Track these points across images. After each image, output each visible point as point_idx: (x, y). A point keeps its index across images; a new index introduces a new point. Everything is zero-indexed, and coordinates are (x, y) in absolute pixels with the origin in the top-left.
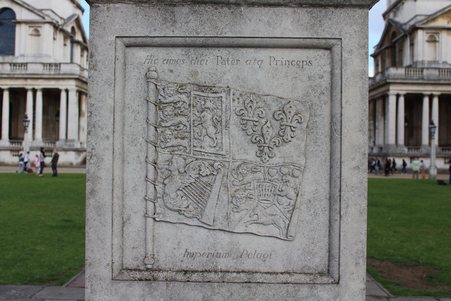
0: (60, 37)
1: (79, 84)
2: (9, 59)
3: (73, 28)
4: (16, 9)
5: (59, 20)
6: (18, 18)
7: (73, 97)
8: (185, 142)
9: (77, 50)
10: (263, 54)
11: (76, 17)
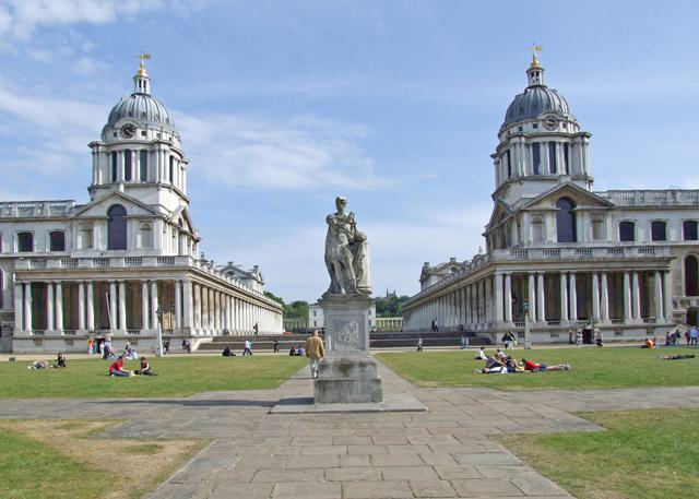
0: (169, 230)
2: (120, 253)
3: (180, 220)
4: (127, 206)
5: (167, 213)
6: (129, 214)
7: (188, 288)
9: (185, 239)
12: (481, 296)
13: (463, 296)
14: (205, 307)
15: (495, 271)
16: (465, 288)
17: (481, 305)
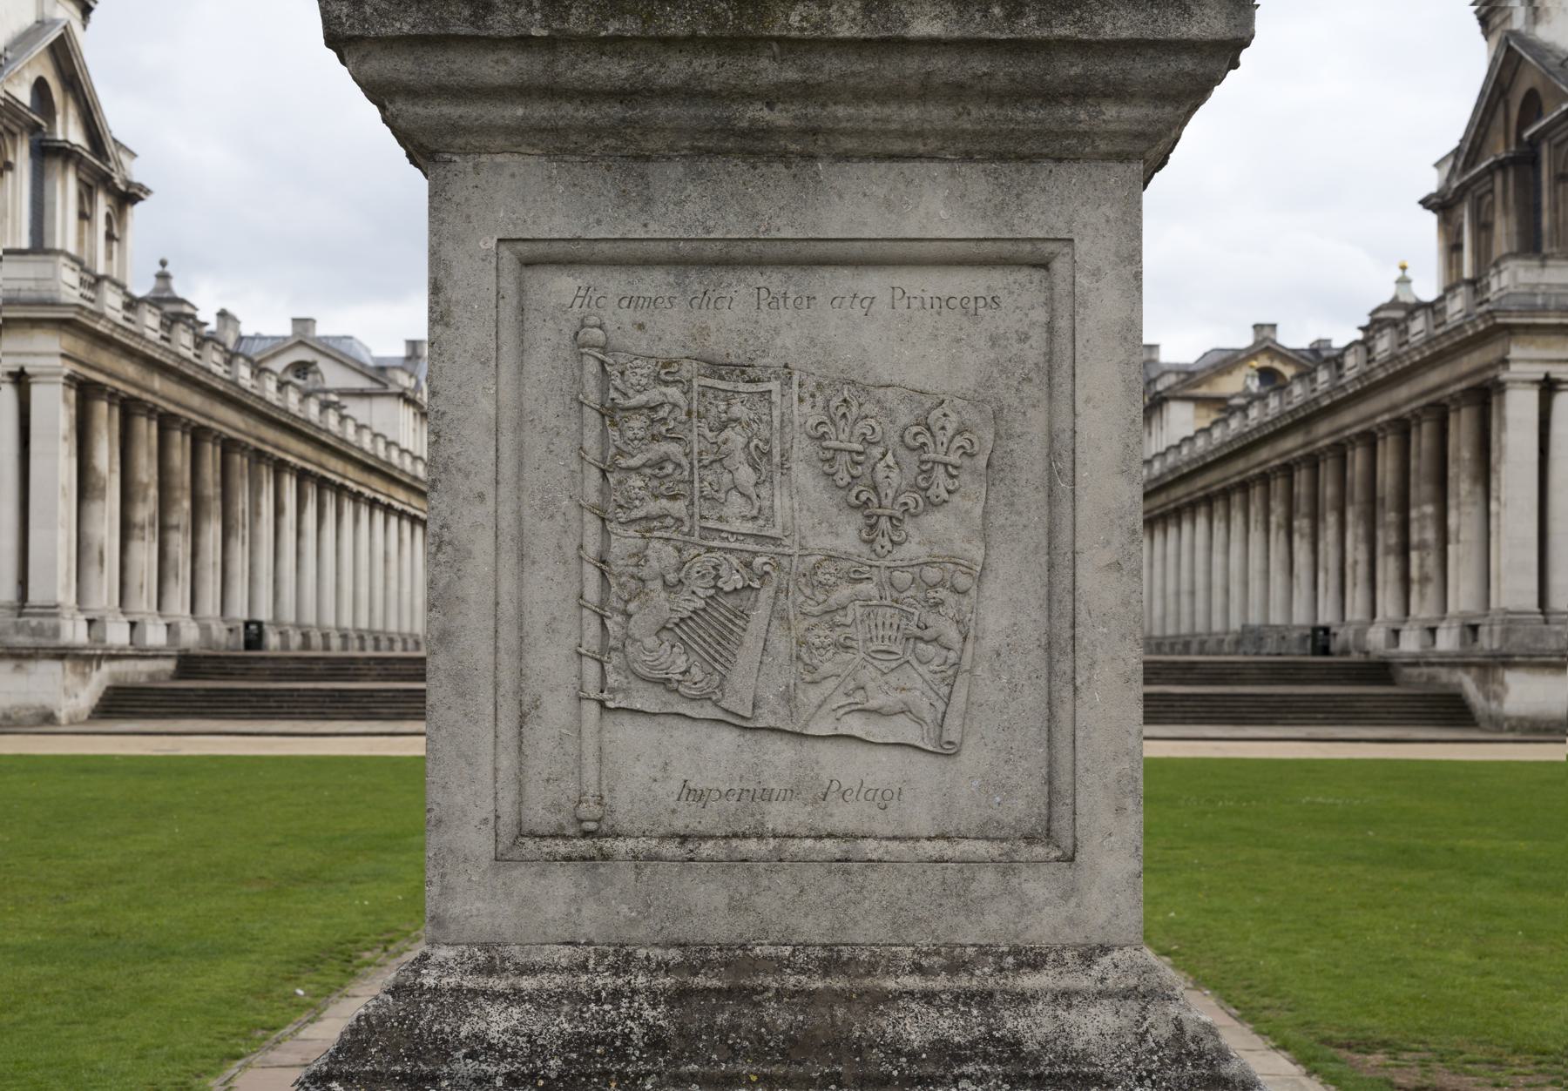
1: (79, 347)
3: (40, 86)
8: (678, 507)
9: (65, 189)
10: (874, 283)
11: (54, 34)
12: (1421, 489)
13: (1329, 491)
14: (145, 512)
15: (1505, 362)
16: (1340, 451)
17: (1425, 532)
